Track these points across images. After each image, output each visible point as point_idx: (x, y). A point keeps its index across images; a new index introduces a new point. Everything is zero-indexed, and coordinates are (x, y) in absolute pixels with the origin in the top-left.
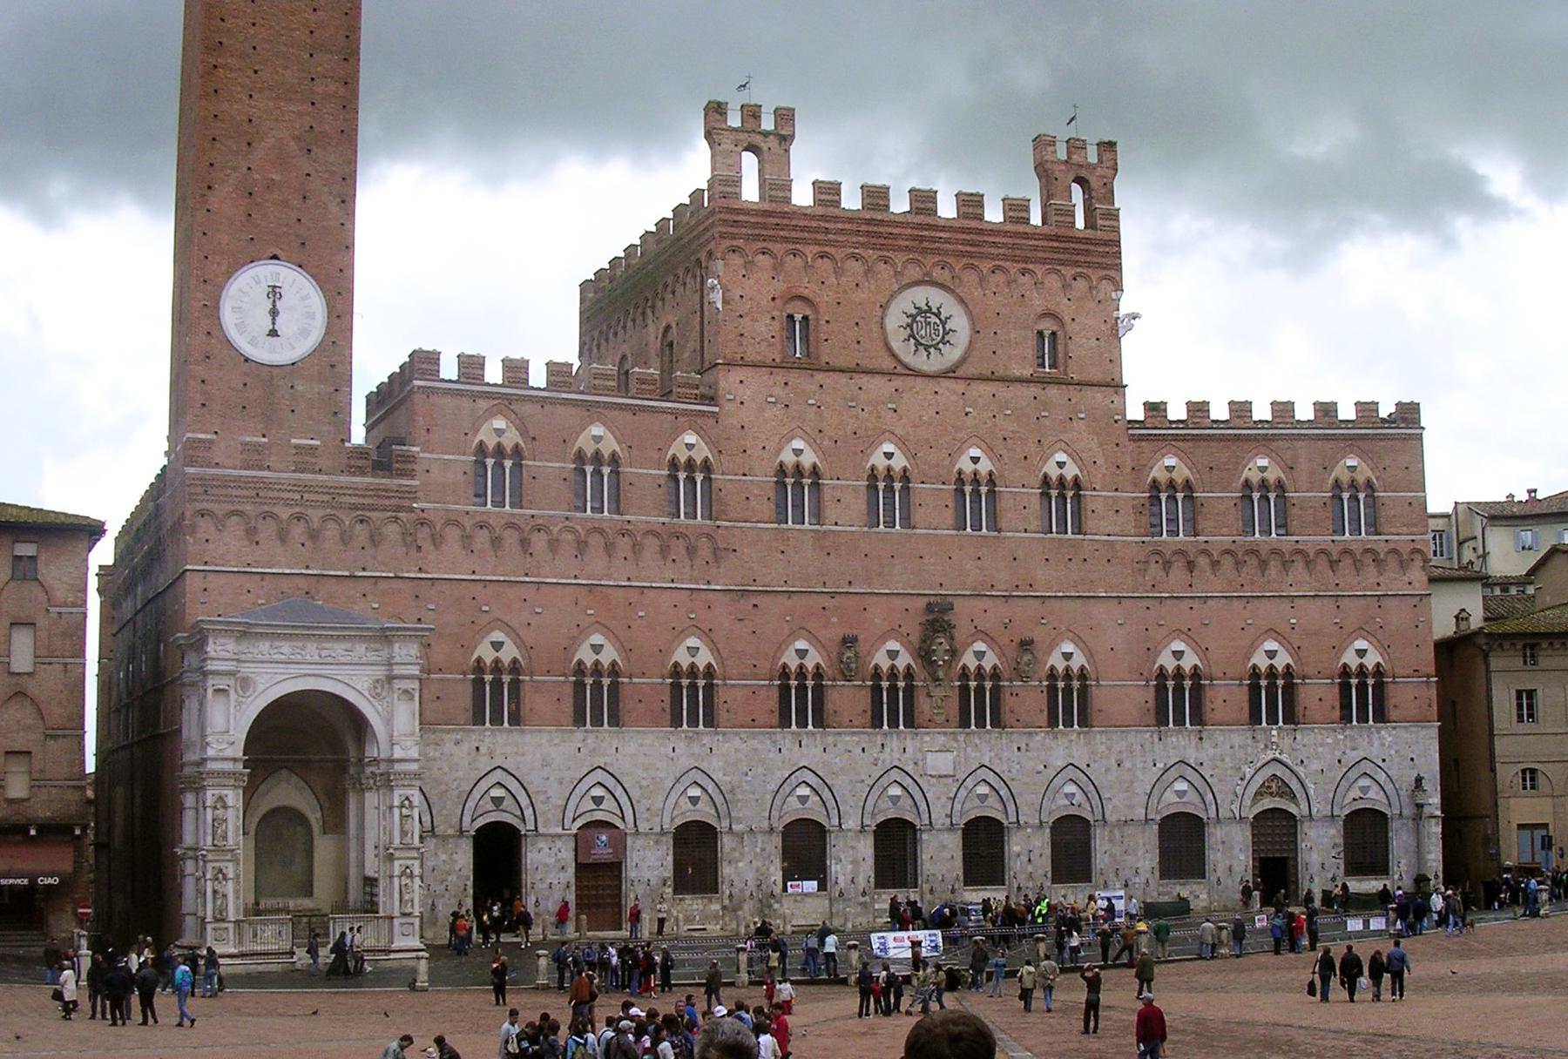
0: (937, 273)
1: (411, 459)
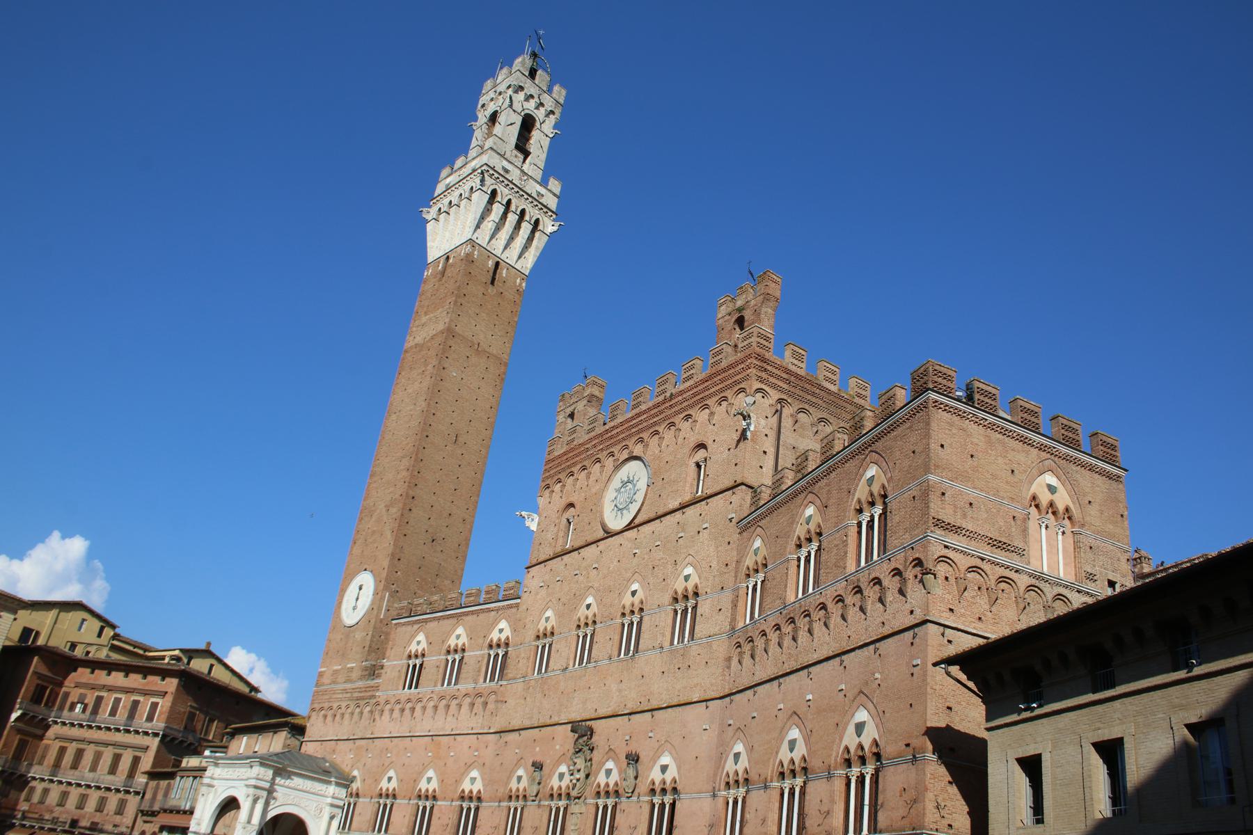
0: (638, 450)
1: (382, 667)
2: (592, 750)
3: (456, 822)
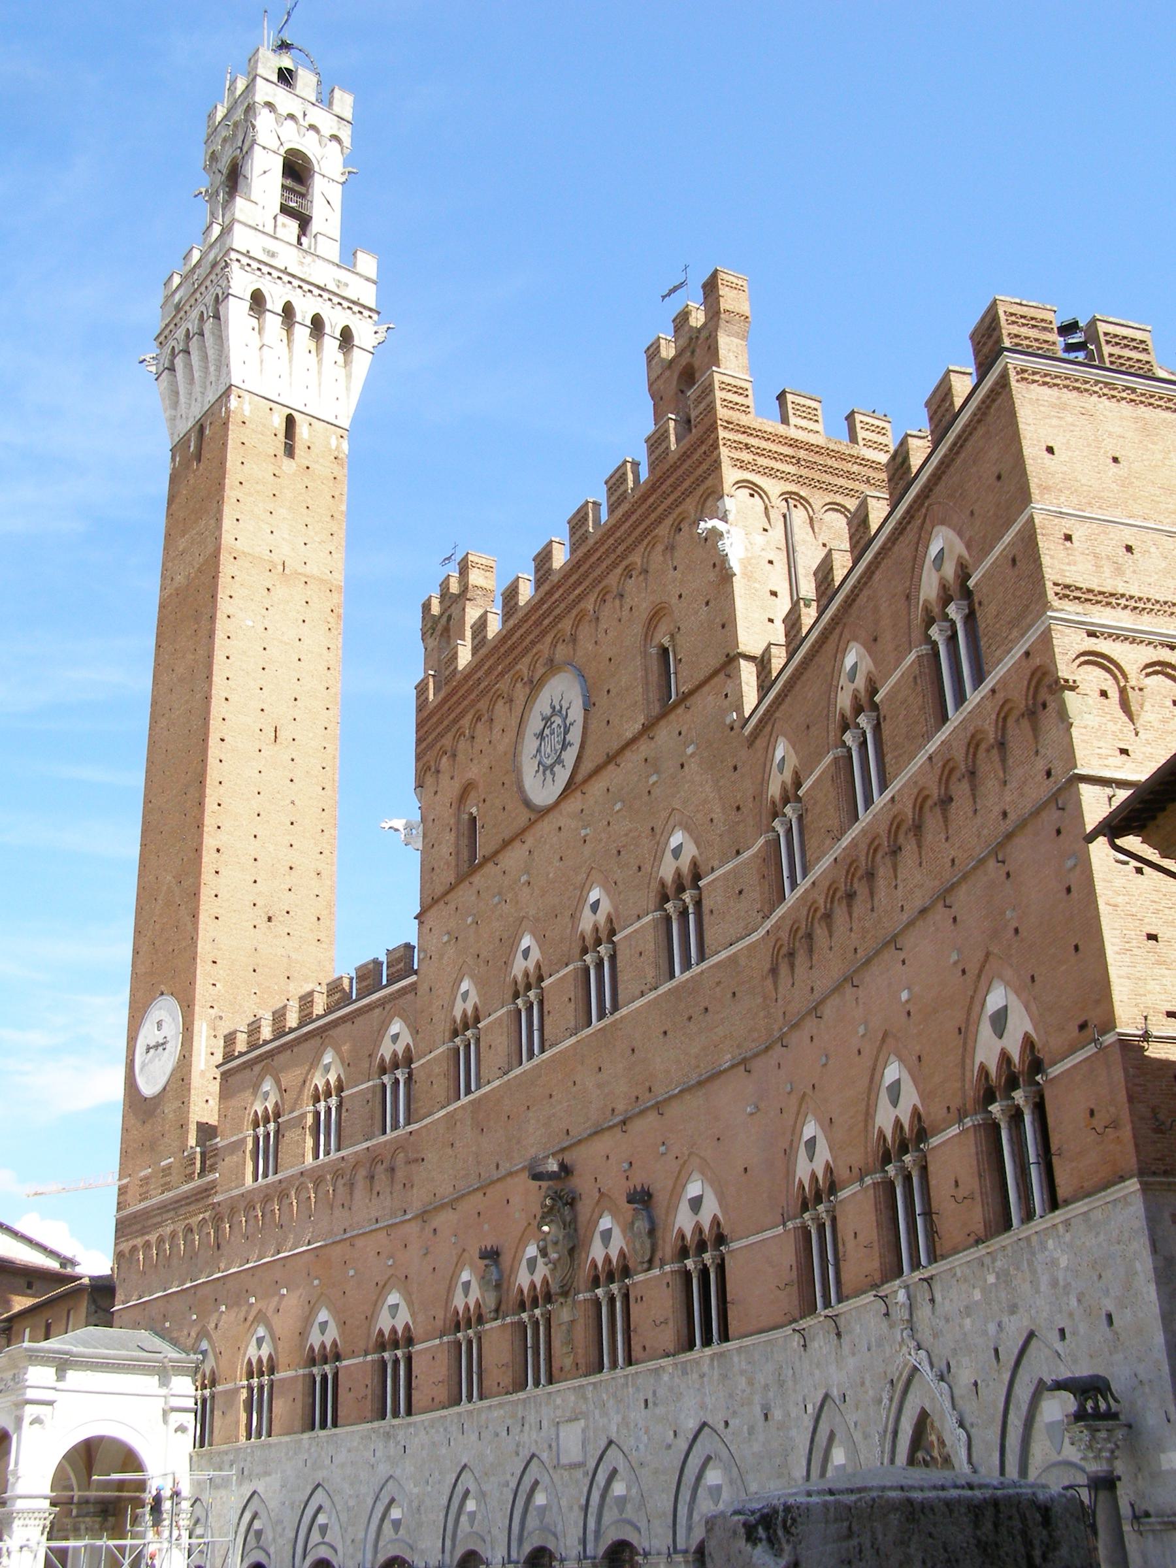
2: (572, 1203)
3: (379, 1392)
